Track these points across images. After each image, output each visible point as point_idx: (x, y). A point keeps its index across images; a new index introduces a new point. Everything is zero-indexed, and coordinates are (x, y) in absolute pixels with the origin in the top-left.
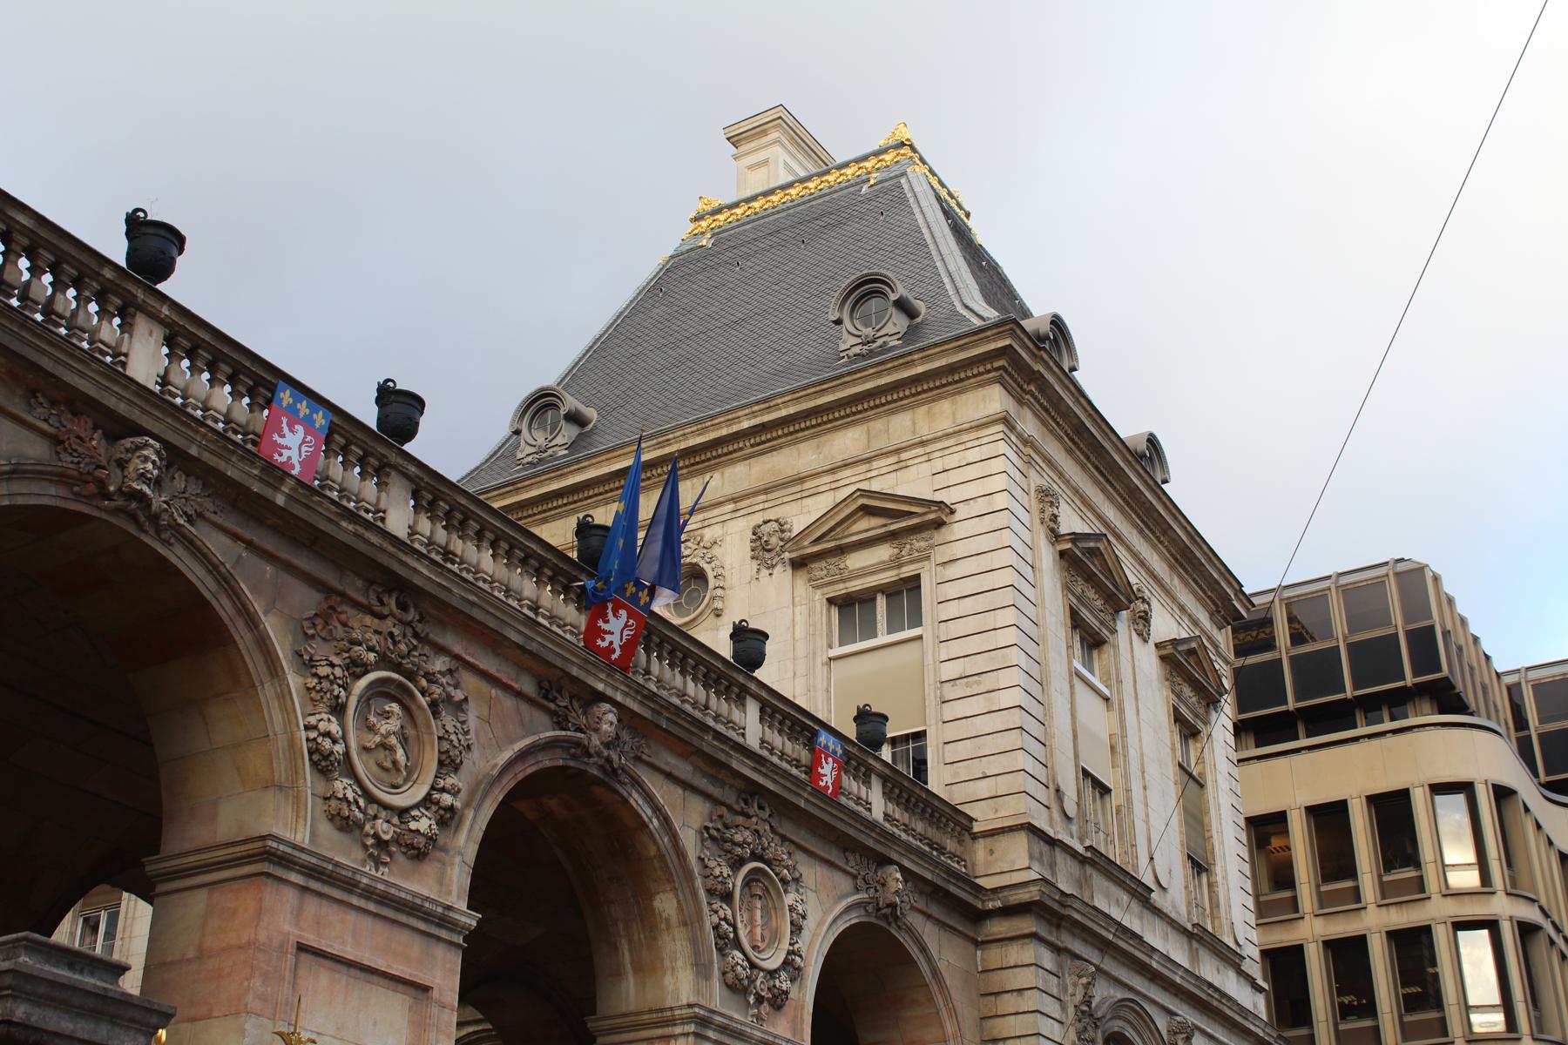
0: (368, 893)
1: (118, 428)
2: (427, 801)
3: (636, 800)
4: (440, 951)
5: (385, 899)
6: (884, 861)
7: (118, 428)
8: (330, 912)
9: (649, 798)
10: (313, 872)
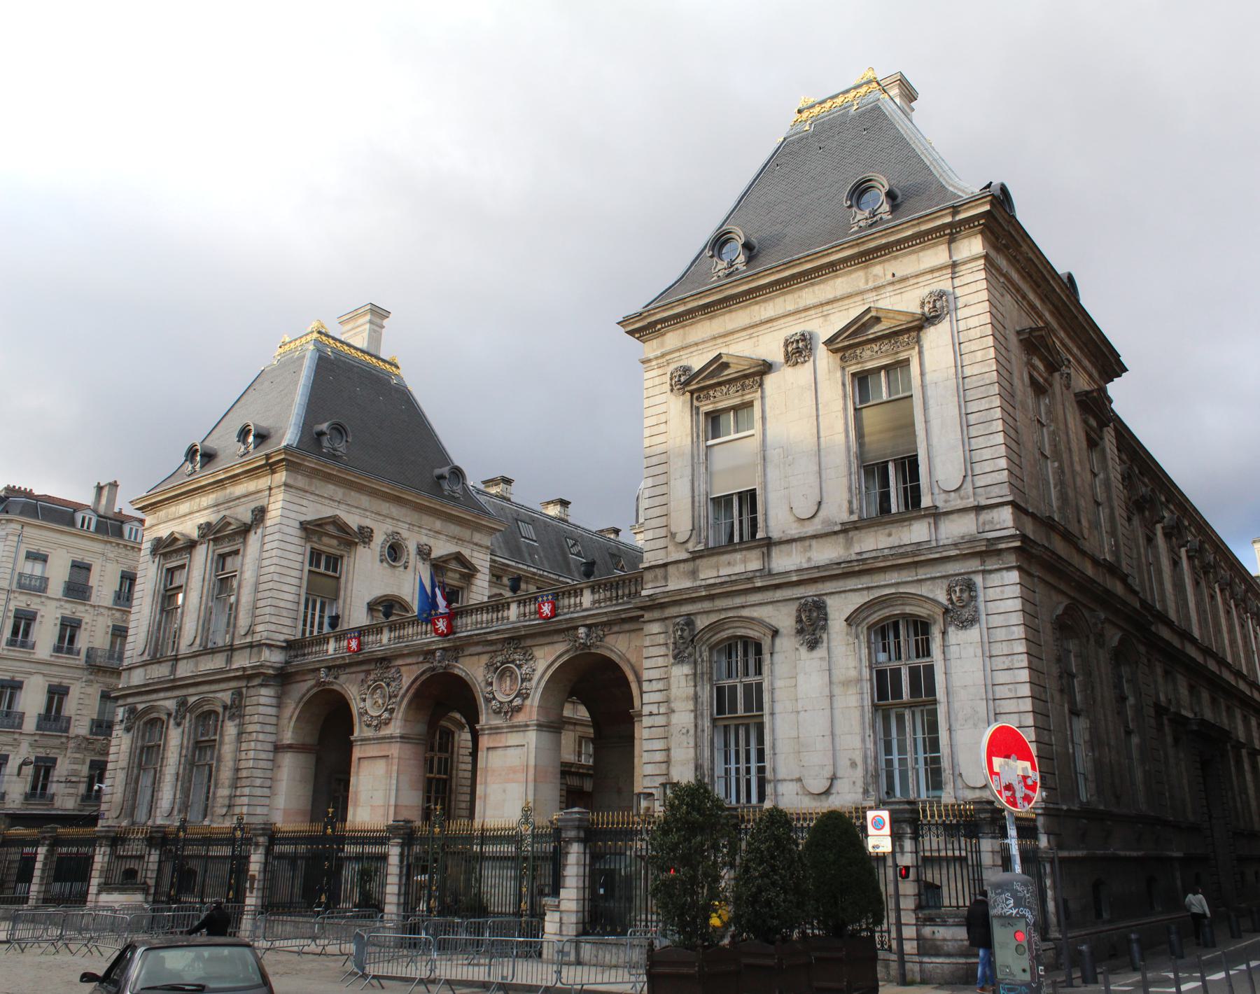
0: (374, 739)
1: (318, 669)
2: (386, 710)
3: (456, 671)
4: (393, 745)
5: (377, 739)
6: (576, 628)
7: (318, 669)
8: (367, 747)
9: (459, 668)
10: (362, 740)
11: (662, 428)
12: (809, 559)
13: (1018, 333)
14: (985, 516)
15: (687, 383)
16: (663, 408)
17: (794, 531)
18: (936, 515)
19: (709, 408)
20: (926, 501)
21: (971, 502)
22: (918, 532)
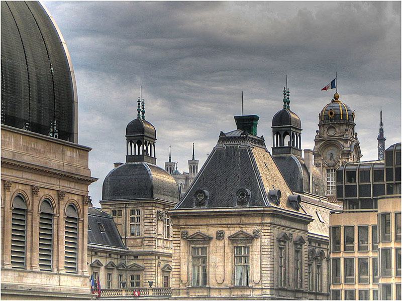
11: (178, 248)
12: (220, 294)
13: (277, 238)
14: (264, 291)
15: (186, 239)
16: (179, 242)
17: (217, 287)
18: (253, 289)
19: (193, 246)
20: (250, 285)
21: (260, 287)
22: (248, 292)
